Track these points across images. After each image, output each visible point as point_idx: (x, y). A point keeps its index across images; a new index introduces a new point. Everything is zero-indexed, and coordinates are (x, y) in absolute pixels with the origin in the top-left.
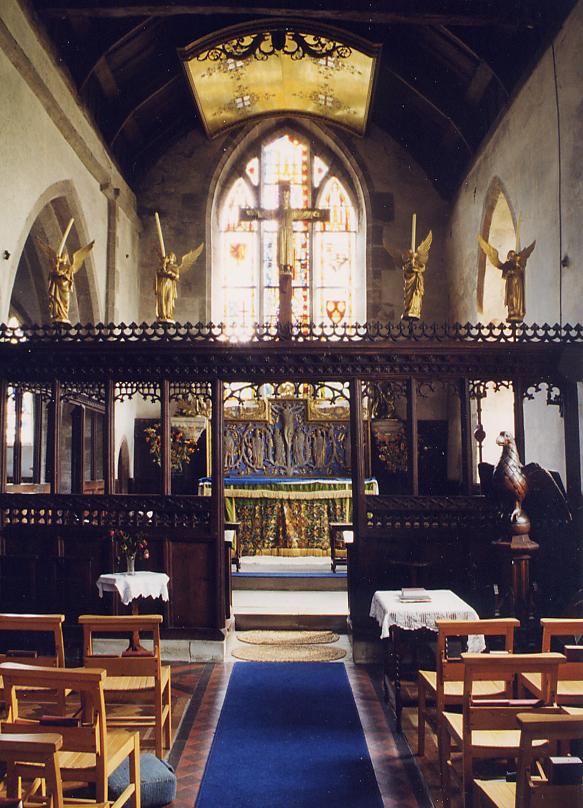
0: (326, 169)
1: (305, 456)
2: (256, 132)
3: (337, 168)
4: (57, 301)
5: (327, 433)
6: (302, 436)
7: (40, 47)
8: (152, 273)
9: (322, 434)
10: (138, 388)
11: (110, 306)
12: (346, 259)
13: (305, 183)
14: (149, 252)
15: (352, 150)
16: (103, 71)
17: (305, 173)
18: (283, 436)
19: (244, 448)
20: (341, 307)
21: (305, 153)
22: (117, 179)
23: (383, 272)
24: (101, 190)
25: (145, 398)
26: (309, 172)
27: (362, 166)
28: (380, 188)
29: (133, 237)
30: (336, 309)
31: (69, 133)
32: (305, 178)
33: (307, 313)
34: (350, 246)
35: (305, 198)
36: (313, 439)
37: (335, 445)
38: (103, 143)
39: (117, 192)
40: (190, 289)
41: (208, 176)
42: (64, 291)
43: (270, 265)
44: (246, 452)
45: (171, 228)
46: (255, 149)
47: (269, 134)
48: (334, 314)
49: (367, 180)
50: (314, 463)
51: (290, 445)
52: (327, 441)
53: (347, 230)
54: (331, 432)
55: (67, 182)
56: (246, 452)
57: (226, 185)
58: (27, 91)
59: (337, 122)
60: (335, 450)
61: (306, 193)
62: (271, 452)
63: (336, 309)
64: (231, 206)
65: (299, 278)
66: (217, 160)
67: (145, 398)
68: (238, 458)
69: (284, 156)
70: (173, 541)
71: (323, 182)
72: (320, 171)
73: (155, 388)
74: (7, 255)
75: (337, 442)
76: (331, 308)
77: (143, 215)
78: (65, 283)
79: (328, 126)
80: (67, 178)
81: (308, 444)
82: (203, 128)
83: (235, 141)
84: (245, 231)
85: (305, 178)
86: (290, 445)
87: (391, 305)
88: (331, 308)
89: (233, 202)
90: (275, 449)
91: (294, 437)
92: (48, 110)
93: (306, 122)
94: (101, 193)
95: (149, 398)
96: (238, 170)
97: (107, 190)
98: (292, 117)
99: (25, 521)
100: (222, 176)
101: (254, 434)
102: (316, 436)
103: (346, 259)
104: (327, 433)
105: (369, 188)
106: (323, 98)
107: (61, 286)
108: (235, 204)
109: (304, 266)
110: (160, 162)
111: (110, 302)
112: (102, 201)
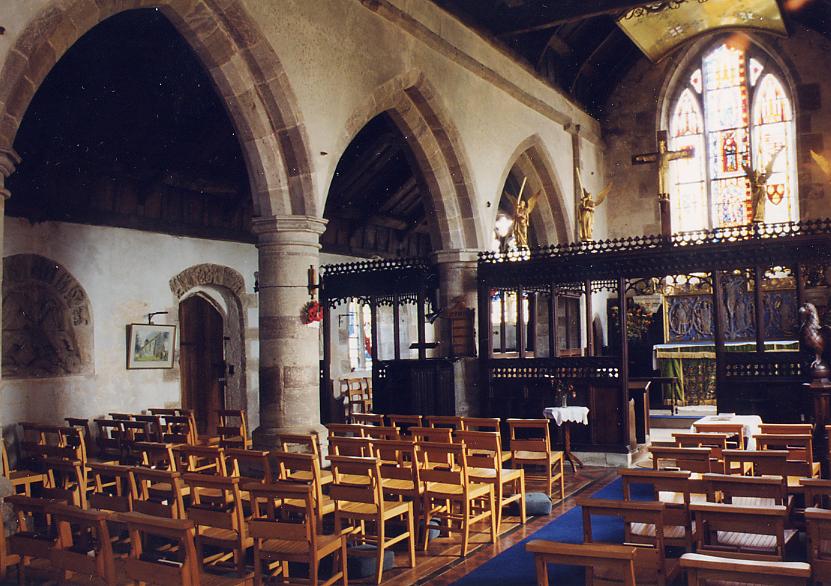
0: (761, 68)
1: (746, 322)
2: (695, 47)
3: (770, 66)
6: (743, 306)
7: (501, 55)
8: (613, 177)
12: (783, 147)
13: (742, 84)
15: (779, 51)
16: (556, 43)
17: (741, 75)
18: (726, 306)
20: (780, 190)
21: (741, 57)
22: (577, 115)
26: (746, 73)
27: (788, 63)
28: (806, 81)
29: (597, 155)
30: (776, 192)
31: (530, 100)
32: (742, 79)
34: (786, 134)
35: (744, 97)
38: (563, 94)
39: (578, 127)
40: (647, 191)
41: (656, 94)
42: (523, 227)
43: (716, 161)
44: (696, 321)
45: (628, 143)
46: (696, 62)
47: (708, 47)
48: (774, 196)
49: (795, 74)
51: (732, 314)
55: (533, 136)
56: (696, 321)
57: (674, 98)
58: (495, 89)
61: (744, 92)
63: (776, 192)
66: (662, 81)
69: (724, 64)
71: (758, 81)
74: (489, 204)
77: (606, 136)
78: (523, 221)
80: (533, 133)
81: (748, 312)
82: (646, 58)
83: (676, 62)
85: (742, 79)
86: (732, 314)
91: (735, 307)
92: (512, 95)
94: (566, 132)
96: (683, 82)
97: (570, 129)
100: (668, 91)
101: (702, 304)
103: (783, 147)
107: (520, 223)
108: (683, 112)
109: (745, 158)
112: (567, 137)
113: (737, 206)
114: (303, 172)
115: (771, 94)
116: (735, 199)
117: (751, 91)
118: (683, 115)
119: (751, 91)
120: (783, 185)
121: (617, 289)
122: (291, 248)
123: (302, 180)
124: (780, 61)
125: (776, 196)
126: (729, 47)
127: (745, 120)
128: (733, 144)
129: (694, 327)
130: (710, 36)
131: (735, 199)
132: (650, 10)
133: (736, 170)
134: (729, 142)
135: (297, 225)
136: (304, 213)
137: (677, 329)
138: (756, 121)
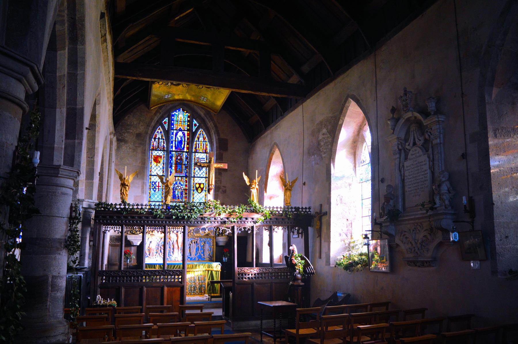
3: (203, 125)
4: (124, 194)
5: (197, 242)
9: (195, 243)
10: (155, 229)
11: (109, 186)
13: (188, 130)
14: (119, 159)
15: (212, 119)
18: (177, 243)
19: (160, 249)
20: (202, 186)
23: (222, 172)
24: (110, 135)
25: (158, 232)
26: (190, 125)
27: (216, 126)
28: (222, 136)
30: (200, 187)
33: (187, 188)
36: (190, 245)
37: (200, 247)
40: (138, 177)
45: (130, 148)
48: (199, 189)
49: (217, 133)
50: (191, 255)
52: (196, 245)
53: (206, 152)
54: (198, 241)
56: (161, 251)
57: (154, 129)
59: (205, 106)
60: (200, 249)
62: (172, 250)
63: (200, 187)
64: (155, 139)
65: (184, 173)
67: (158, 232)
68: (157, 253)
70: (167, 287)
71: (197, 130)
72: (195, 125)
73: (162, 229)
75: (201, 246)
76: (197, 186)
79: (202, 108)
84: (161, 150)
87: (225, 187)
88: (197, 186)
89: (156, 136)
90: (173, 249)
93: (192, 104)
95: (159, 232)
98: (185, 102)
99: (8, 282)
102: (192, 243)
104: (197, 242)
105: (218, 136)
106: (204, 100)
107: (125, 188)
108: (157, 138)
109: (186, 167)
110: (127, 118)
111: (109, 184)
113: (180, 191)
114: (78, 139)
115: (201, 139)
116: (179, 187)
117: (192, 135)
118: (157, 140)
119: (192, 135)
120: (203, 184)
121: (183, 232)
122: (64, 190)
123: (76, 144)
124: (210, 124)
125: (200, 189)
126: (183, 110)
127: (188, 148)
128: (181, 159)
129: (159, 254)
130: (179, 102)
131: (179, 187)
132: (172, 84)
133: (182, 173)
134: (179, 158)
135: (71, 174)
136: (72, 165)
137: (149, 255)
138: (194, 150)
